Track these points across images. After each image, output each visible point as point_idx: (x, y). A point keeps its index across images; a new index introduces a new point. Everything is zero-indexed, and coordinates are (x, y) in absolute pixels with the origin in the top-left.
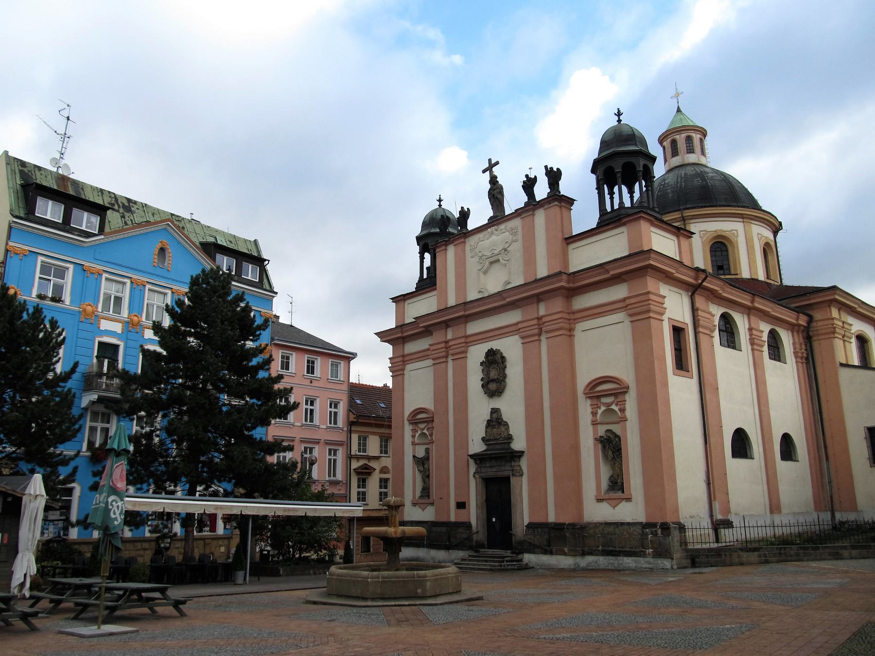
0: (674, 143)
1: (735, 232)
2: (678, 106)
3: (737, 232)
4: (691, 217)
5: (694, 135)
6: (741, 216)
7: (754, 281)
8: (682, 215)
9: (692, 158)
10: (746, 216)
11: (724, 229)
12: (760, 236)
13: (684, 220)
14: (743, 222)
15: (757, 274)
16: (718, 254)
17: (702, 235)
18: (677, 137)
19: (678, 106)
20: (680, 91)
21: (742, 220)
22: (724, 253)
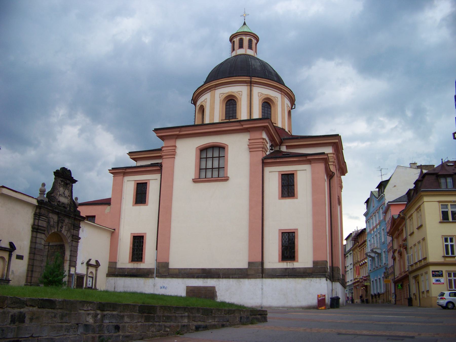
0: (241, 41)
1: (277, 98)
2: (245, 22)
3: (278, 99)
4: (255, 82)
5: (253, 39)
6: (280, 90)
7: (283, 130)
8: (251, 80)
9: (250, 52)
10: (284, 91)
11: (272, 95)
12: (287, 105)
13: (251, 83)
14: (281, 94)
15: (285, 126)
16: (266, 109)
17: (259, 95)
18: (244, 37)
19: (245, 22)
20: (246, 13)
21: (280, 92)
22: (269, 110)
